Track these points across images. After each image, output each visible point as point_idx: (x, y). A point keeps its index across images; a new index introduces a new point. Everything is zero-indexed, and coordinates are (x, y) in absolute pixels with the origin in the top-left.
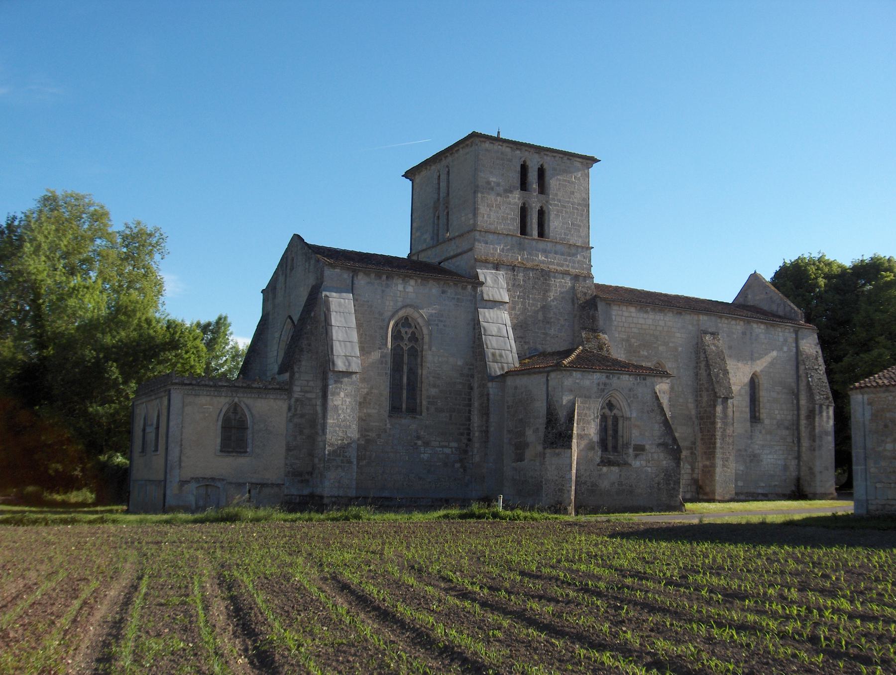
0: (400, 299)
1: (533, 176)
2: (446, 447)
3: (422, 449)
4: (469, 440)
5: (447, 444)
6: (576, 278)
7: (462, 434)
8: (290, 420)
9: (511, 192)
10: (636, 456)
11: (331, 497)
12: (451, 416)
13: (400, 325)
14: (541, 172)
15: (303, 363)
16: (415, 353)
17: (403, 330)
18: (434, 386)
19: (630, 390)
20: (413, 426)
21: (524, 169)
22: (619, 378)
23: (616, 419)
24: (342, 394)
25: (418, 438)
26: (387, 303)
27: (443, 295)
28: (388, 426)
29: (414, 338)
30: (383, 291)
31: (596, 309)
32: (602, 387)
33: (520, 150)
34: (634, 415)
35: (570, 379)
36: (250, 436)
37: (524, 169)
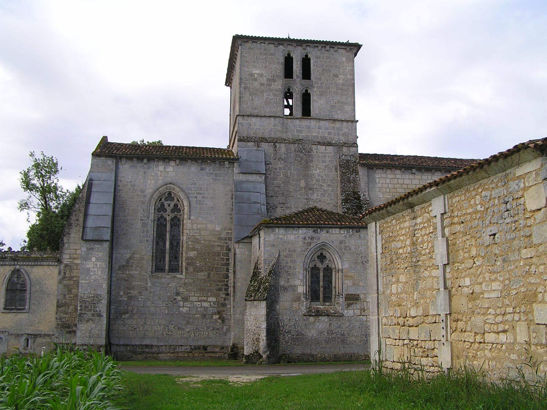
0: (160, 178)
1: (297, 67)
2: (204, 301)
3: (181, 303)
4: (228, 294)
5: (205, 299)
6: (339, 146)
7: (220, 290)
8: (60, 282)
9: (274, 81)
10: (349, 305)
11: (82, 345)
12: (209, 274)
13: (163, 199)
14: (306, 62)
15: (72, 235)
16: (177, 223)
17: (166, 204)
18: (193, 249)
19: (341, 243)
20: (173, 284)
21: (288, 61)
22: (327, 232)
23: (328, 271)
24: (94, 259)
25: (178, 294)
26: (149, 182)
27: (202, 172)
28: (149, 284)
29: (176, 209)
30: (145, 173)
31: (357, 173)
32: (308, 240)
33: (283, 44)
34: (346, 266)
35: (272, 235)
36: (28, 296)
37: (288, 61)
